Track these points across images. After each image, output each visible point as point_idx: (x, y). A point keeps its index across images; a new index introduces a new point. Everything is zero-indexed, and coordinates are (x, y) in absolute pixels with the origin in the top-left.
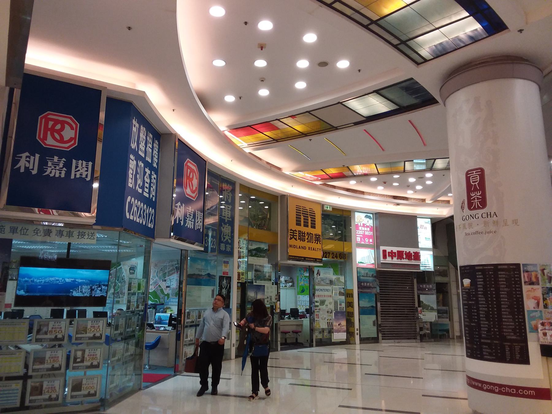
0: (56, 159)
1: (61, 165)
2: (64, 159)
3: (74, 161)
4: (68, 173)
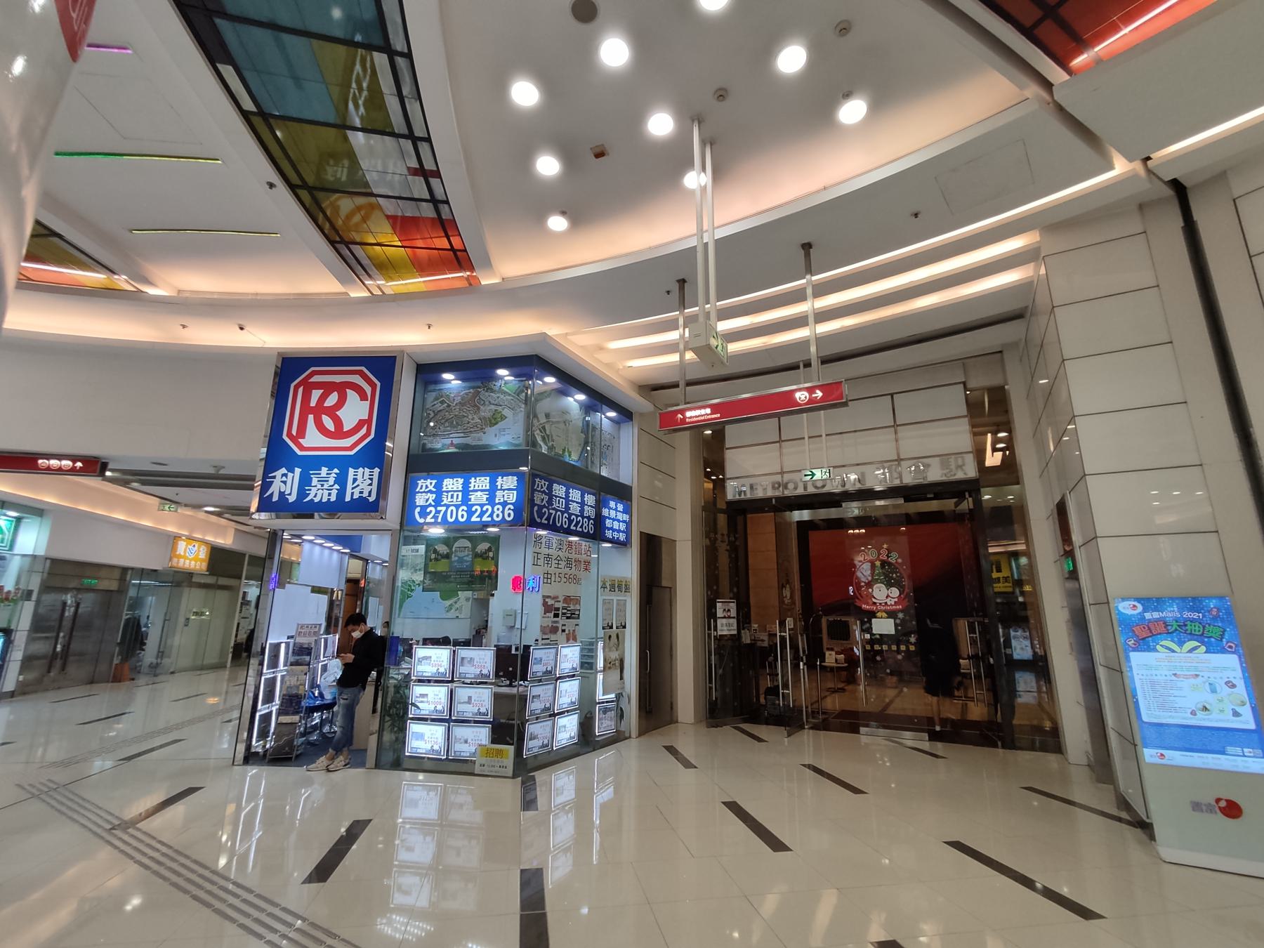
0: (324, 470)
1: (331, 482)
2: (336, 471)
3: (351, 471)
4: (341, 493)
